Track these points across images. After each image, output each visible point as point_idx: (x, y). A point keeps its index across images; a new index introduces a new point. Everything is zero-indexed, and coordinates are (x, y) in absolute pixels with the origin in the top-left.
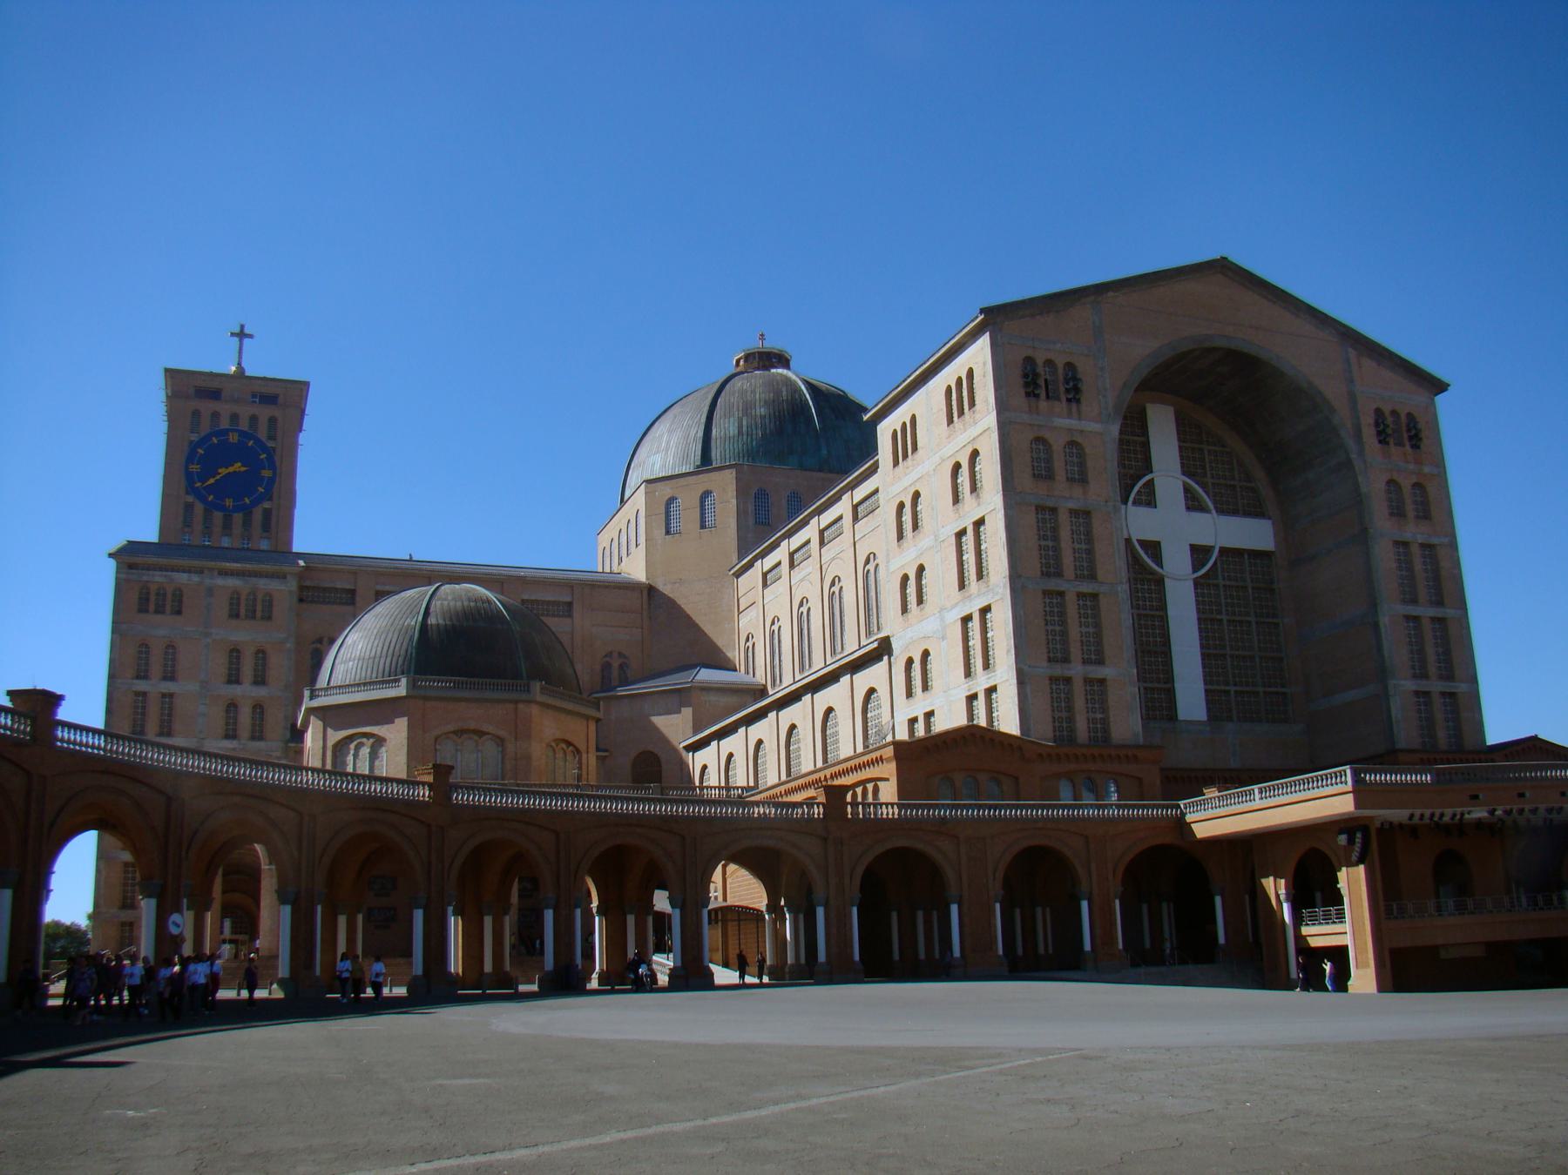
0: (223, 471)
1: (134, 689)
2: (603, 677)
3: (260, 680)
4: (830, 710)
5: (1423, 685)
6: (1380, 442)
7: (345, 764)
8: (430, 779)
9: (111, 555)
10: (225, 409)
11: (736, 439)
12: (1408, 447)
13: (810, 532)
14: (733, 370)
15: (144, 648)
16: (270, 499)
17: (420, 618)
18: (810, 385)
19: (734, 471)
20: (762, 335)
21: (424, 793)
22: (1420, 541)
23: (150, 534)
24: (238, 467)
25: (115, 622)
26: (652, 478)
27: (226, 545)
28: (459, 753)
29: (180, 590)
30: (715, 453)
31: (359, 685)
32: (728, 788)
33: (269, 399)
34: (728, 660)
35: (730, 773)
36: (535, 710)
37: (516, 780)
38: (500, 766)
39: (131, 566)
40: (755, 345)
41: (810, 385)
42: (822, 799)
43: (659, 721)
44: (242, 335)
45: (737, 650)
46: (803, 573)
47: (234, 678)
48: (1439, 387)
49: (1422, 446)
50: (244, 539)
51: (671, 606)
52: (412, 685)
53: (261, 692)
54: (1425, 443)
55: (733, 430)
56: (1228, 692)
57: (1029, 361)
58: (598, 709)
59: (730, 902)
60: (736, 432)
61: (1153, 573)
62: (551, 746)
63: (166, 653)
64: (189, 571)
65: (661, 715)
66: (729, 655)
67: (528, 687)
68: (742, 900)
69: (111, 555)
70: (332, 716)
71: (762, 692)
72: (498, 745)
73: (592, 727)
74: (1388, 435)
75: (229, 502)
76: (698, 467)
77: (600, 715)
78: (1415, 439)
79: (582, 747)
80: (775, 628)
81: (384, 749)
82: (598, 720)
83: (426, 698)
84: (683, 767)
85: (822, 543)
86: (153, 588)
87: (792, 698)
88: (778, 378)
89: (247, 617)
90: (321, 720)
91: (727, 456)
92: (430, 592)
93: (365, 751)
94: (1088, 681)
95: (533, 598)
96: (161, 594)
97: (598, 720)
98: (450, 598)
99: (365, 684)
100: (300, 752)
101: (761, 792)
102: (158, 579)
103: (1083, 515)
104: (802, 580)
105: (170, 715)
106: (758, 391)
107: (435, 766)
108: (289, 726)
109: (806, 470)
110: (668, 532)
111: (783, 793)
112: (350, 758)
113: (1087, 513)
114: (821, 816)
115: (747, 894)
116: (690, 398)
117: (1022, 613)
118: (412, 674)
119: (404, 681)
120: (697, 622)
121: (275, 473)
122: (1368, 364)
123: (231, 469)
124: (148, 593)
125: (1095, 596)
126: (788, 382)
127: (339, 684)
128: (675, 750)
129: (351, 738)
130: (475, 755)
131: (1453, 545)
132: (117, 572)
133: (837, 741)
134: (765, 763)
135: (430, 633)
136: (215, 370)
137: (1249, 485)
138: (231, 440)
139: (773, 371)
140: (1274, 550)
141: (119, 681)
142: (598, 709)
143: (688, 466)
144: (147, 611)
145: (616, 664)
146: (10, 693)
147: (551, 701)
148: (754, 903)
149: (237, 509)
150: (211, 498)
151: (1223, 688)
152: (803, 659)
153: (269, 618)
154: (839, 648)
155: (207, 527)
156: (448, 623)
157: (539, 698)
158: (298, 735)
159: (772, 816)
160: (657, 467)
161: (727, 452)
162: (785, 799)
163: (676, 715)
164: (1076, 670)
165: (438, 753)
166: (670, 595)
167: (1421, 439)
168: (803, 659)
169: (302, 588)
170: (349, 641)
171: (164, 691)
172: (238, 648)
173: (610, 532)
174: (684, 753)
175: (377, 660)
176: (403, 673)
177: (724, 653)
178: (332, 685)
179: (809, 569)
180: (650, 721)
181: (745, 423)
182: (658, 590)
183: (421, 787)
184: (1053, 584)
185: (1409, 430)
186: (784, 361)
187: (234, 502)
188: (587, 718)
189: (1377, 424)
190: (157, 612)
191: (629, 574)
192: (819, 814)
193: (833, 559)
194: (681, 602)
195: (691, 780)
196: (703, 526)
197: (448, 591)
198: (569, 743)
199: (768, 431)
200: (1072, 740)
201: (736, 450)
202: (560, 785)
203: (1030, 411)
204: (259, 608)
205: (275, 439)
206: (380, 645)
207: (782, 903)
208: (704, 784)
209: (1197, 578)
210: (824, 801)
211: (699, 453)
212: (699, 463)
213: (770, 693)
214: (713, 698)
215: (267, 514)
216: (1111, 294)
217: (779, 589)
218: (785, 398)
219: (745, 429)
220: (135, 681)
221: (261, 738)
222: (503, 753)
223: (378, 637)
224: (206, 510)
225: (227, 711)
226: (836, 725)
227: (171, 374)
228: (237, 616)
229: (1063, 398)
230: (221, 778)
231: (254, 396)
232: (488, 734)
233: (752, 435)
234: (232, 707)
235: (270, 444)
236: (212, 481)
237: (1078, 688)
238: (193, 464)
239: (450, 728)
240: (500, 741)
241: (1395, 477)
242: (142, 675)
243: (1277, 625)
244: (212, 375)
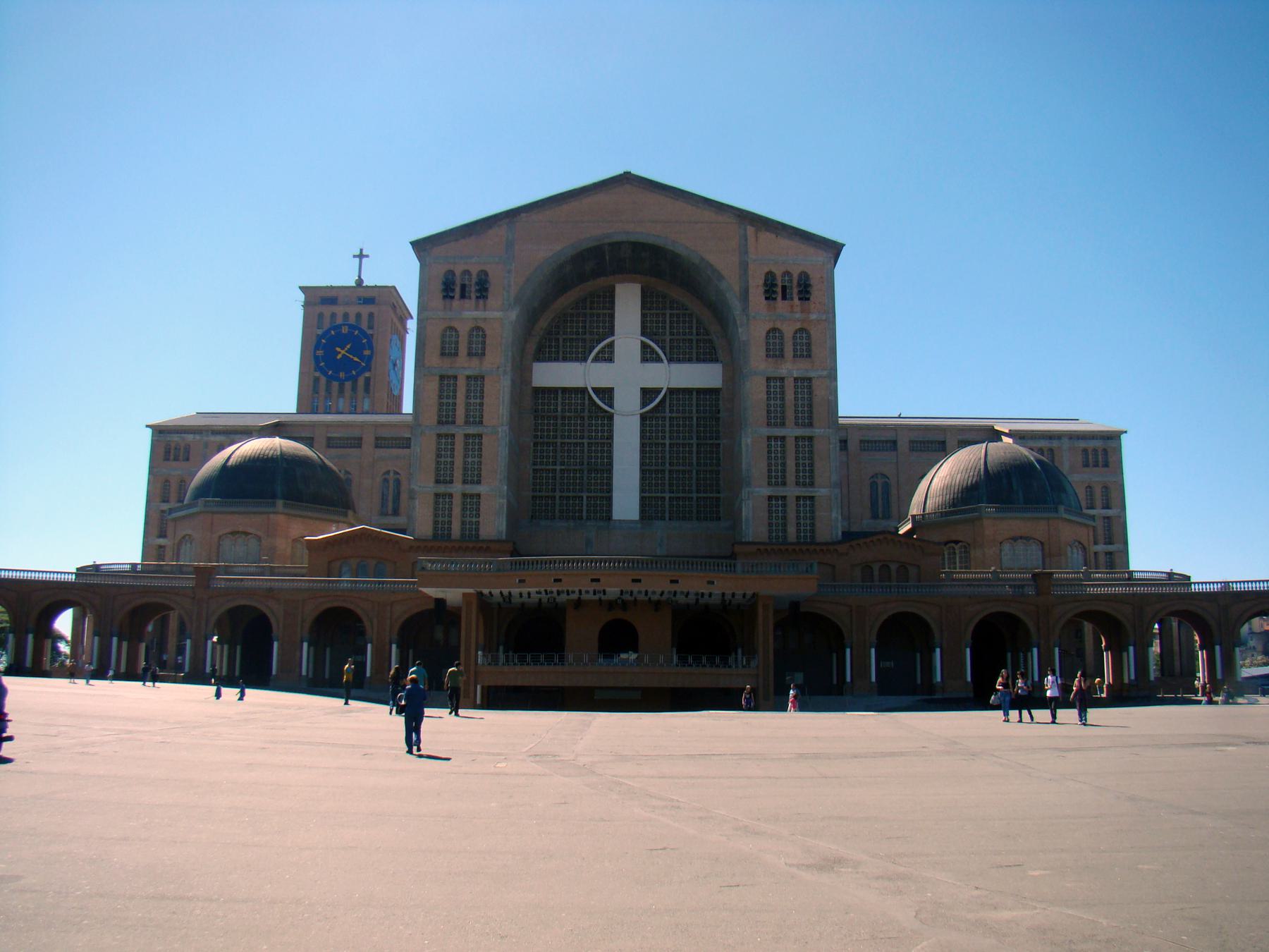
5: (780, 491)
6: (767, 298)
10: (339, 310)
12: (796, 301)
16: (370, 370)
22: (795, 376)
33: (369, 301)
48: (834, 249)
49: (811, 299)
54: (815, 293)
56: (664, 498)
57: (452, 273)
61: (606, 412)
69: (147, 426)
74: (775, 292)
75: (342, 375)
78: (805, 290)
86: (173, 445)
94: (464, 495)
102: (176, 439)
103: (477, 380)
113: (483, 378)
117: (419, 450)
122: (766, 237)
124: (170, 449)
125: (480, 436)
131: (832, 376)
132: (152, 436)
137: (706, 337)
138: (343, 331)
140: (721, 387)
144: (168, 460)
149: (347, 379)
150: (330, 372)
151: (659, 495)
164: (457, 488)
167: (808, 292)
184: (445, 430)
185: (799, 285)
187: (346, 373)
189: (765, 284)
200: (449, 535)
203: (445, 308)
209: (647, 412)
215: (368, 380)
216: (523, 215)
220: (162, 504)
229: (473, 296)
231: (360, 299)
232: (251, 534)
235: (370, 332)
236: (356, 359)
237: (457, 501)
238: (318, 350)
239: (228, 530)
240: (259, 539)
241: (778, 325)
243: (719, 444)
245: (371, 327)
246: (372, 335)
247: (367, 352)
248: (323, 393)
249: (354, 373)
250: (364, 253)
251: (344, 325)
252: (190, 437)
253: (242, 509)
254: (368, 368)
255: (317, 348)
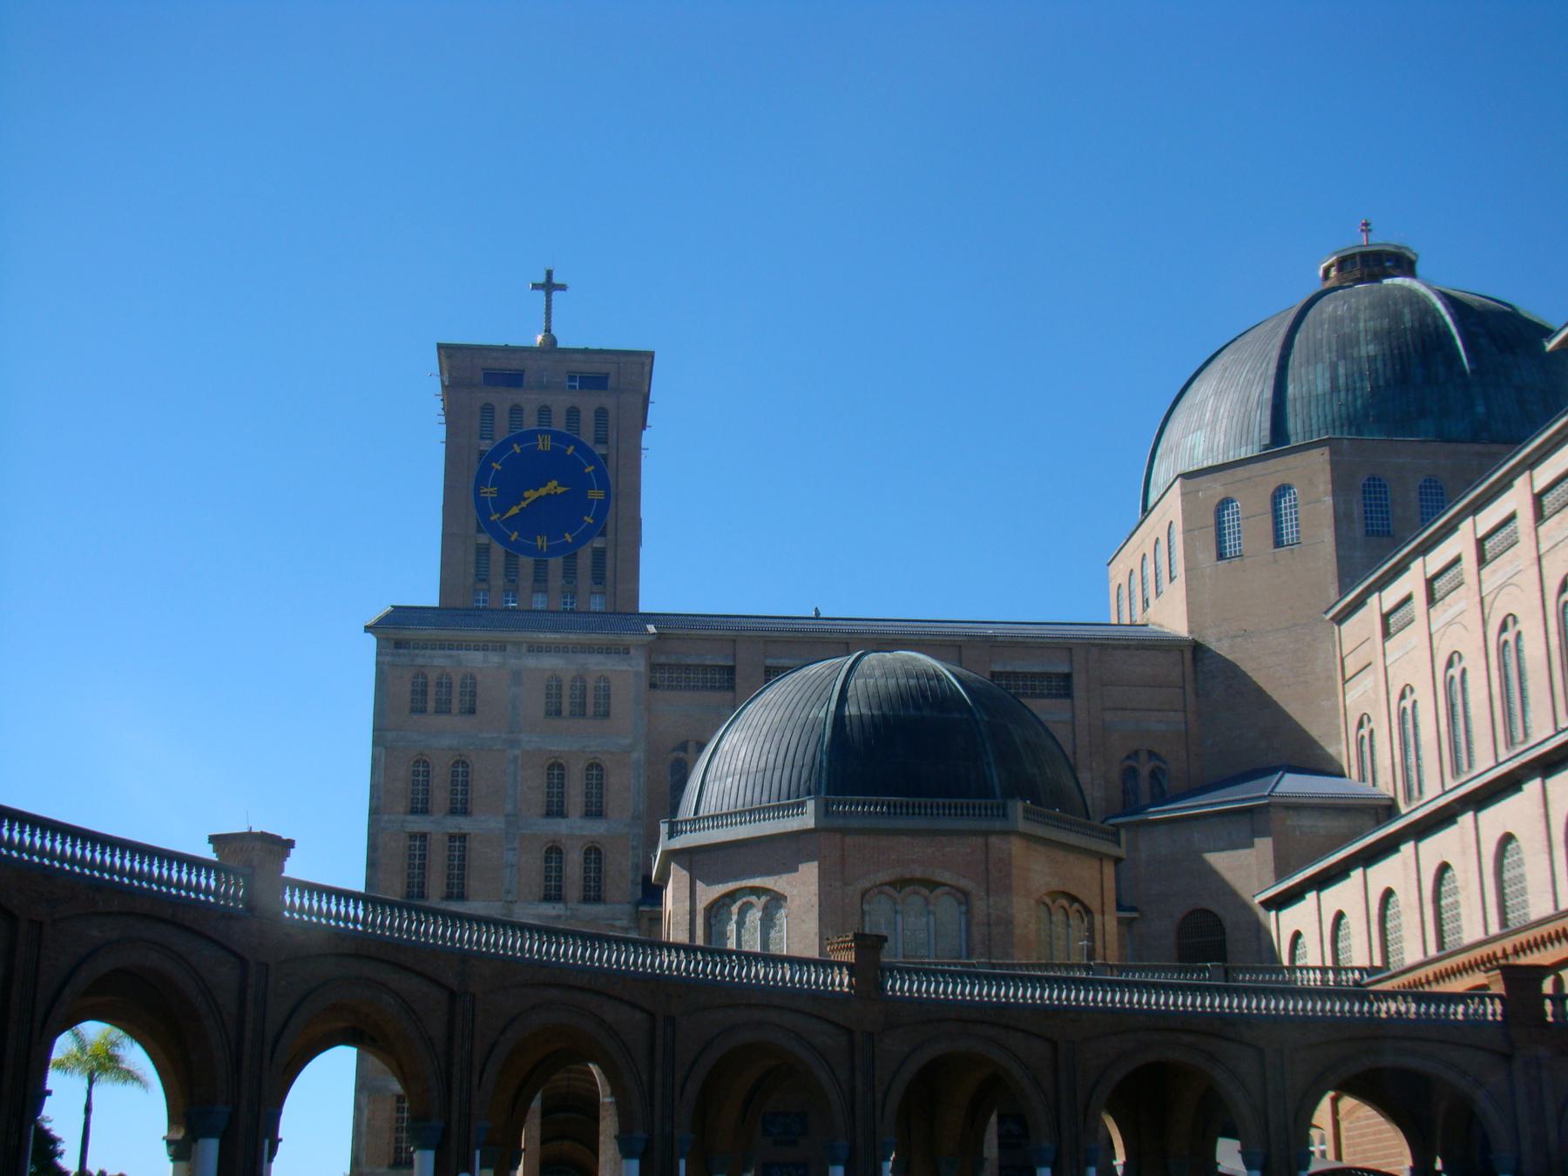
0: (531, 495)
1: (407, 830)
2: (1124, 792)
3: (595, 811)
4: (1507, 839)
7: (723, 936)
8: (850, 957)
9: (368, 629)
10: (529, 401)
11: (1328, 397)
13: (1460, 543)
14: (1319, 286)
15: (422, 767)
16: (603, 534)
17: (833, 707)
18: (1452, 302)
19: (1326, 450)
20: (1366, 224)
21: (841, 980)
23: (428, 595)
24: (552, 487)
25: (378, 729)
26: (1191, 469)
27: (540, 607)
28: (899, 917)
29: (473, 677)
30: (1294, 425)
31: (742, 813)
32: (1337, 969)
33: (595, 382)
34: (1330, 759)
35: (1340, 945)
36: (1016, 846)
37: (990, 958)
38: (964, 936)
39: (399, 644)
40: (1355, 241)
41: (1452, 302)
42: (1498, 988)
43: (1220, 861)
44: (549, 286)
45: (1344, 743)
46: (1451, 612)
47: (556, 809)
50: (566, 597)
51: (1231, 674)
52: (824, 811)
53: (596, 829)
55: (1322, 385)
58: (1118, 843)
59: (1348, 1160)
60: (1328, 385)
62: (1046, 905)
63: (454, 774)
64: (483, 647)
65: (1223, 850)
66: (1331, 750)
67: (1005, 808)
68: (1367, 1159)
69: (368, 629)
70: (699, 862)
71: (1388, 810)
72: (960, 904)
73: (1109, 870)
75: (541, 542)
76: (1266, 447)
77: (1121, 852)
79: (1094, 904)
80: (1407, 703)
81: (783, 912)
82: (1117, 861)
83: (845, 832)
84: (1261, 934)
85: (1482, 561)
86: (432, 677)
87: (1442, 819)
88: (1396, 292)
89: (572, 714)
90: (685, 869)
91: (1315, 427)
92: (847, 666)
93: (754, 916)
95: (1009, 669)
96: (445, 684)
97: (1117, 861)
98: (877, 673)
99: (751, 812)
100: (657, 919)
101: (1392, 977)
102: (438, 662)
104: (1449, 624)
105: (462, 867)
106: (1362, 316)
107: (860, 938)
108: (640, 879)
109: (1449, 441)
110: (1221, 556)
111: (1431, 978)
112: (732, 927)
114: (1499, 1018)
115: (1377, 1149)
116: (1248, 337)
118: (823, 795)
119: (810, 805)
120: (1275, 697)
121: (608, 495)
123: (543, 491)
124: (426, 685)
126: (1413, 298)
127: (712, 813)
128: (1246, 907)
129: (731, 896)
130: (924, 920)
132: (379, 654)
133: (1523, 892)
134: (1398, 928)
135: (848, 728)
136: (513, 343)
138: (541, 447)
139: (1387, 281)
141: (386, 817)
142: (1118, 843)
143: (1250, 447)
144: (423, 711)
145: (1145, 769)
146: (215, 840)
147: (1041, 831)
148: (1389, 1164)
149: (553, 551)
150: (514, 536)
152: (1458, 751)
153: (607, 714)
154: (1519, 735)
155: (513, 581)
156: (875, 712)
157: (1022, 825)
158: (652, 893)
159: (1412, 1016)
160: (1199, 451)
161: (1314, 421)
162: (1436, 988)
163: (1247, 851)
165: (867, 918)
166: (1229, 657)
168: (1458, 751)
169: (654, 667)
170: (726, 745)
171: (451, 831)
172: (561, 761)
173: (1128, 559)
174: (1261, 912)
175: (768, 774)
176: (809, 793)
177: (1321, 748)
178: (701, 814)
179: (1461, 605)
180: (1205, 863)
181: (1341, 371)
182: (1209, 649)
183: (837, 971)
186: (1403, 263)
188: (1101, 857)
190: (438, 711)
191: (1161, 626)
192: (1494, 1014)
193: (1502, 587)
194: (1247, 667)
195: (1274, 955)
196: (1278, 543)
197: (874, 662)
198: (1073, 899)
199: (1381, 382)
201: (1329, 418)
202: (1059, 966)
204: (590, 700)
205: (606, 443)
206: (773, 750)
207: (1439, 1165)
208: (1298, 963)
210: (1503, 992)
211: (1267, 425)
212: (1267, 441)
213: (1404, 810)
214: (1307, 822)
215: (599, 556)
217: (1410, 640)
218: (1409, 325)
219: (1342, 381)
220: (411, 818)
221: (598, 899)
222: (969, 914)
223: (769, 737)
224: (507, 554)
225: (547, 859)
226: (1520, 863)
227: (448, 352)
228: (559, 713)
230: (531, 961)
231: (572, 378)
233: (1355, 389)
234: (554, 852)
235: (600, 450)
236: (515, 510)
239: (883, 876)
240: (964, 897)
242: (420, 807)
244: (506, 349)
245: (602, 440)
246: (605, 457)
247: (596, 494)
248: (498, 581)
249: (568, 538)
250: (556, 280)
251: (543, 432)
252: (475, 659)
253: (922, 823)
254: (600, 529)
255: (480, 481)
